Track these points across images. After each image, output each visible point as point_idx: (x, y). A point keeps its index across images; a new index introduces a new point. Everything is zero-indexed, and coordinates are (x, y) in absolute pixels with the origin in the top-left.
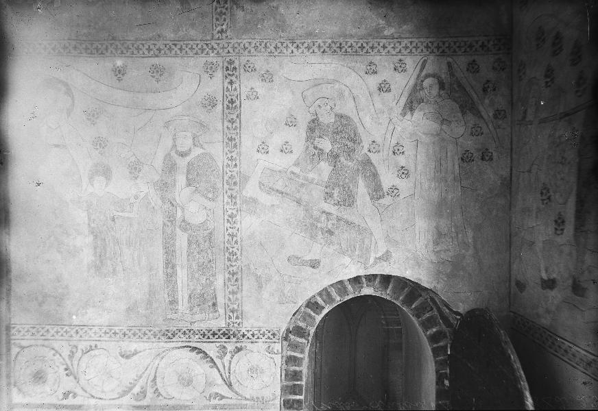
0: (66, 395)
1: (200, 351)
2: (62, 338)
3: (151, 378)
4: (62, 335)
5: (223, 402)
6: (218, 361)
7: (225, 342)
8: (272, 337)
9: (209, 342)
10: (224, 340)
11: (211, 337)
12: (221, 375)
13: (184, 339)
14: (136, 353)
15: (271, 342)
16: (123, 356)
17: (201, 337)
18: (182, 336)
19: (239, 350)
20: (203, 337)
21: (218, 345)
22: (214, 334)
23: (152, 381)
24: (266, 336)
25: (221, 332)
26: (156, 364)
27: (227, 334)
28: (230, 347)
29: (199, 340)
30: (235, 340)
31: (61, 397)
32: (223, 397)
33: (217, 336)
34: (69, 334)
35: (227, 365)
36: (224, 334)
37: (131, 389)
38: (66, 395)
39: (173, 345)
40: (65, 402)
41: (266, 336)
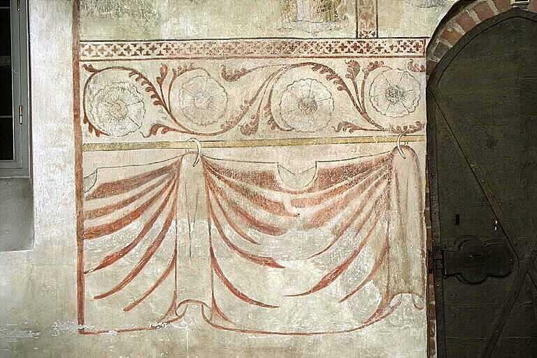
0: (153, 130)
1: (325, 69)
2: (147, 57)
3: (265, 103)
4: (148, 54)
5: (356, 134)
6: (348, 82)
7: (357, 57)
8: (414, 50)
9: (336, 57)
10: (355, 54)
11: (339, 50)
12: (353, 101)
13: (305, 54)
14: (245, 72)
15: (414, 57)
16: (226, 78)
17: (327, 51)
18: (302, 50)
19: (375, 66)
20: (330, 51)
21: (349, 60)
22: (343, 47)
23: (265, 109)
24: (408, 49)
25: (352, 44)
26: (270, 86)
27: (359, 47)
28: (364, 63)
29: (325, 55)
30: (368, 54)
31: (147, 132)
32: (354, 128)
33: (346, 50)
34: (157, 52)
35: (359, 87)
36: (355, 47)
37: (239, 120)
38: (153, 130)
39: (291, 61)
40: (153, 139)
41: (408, 49)
